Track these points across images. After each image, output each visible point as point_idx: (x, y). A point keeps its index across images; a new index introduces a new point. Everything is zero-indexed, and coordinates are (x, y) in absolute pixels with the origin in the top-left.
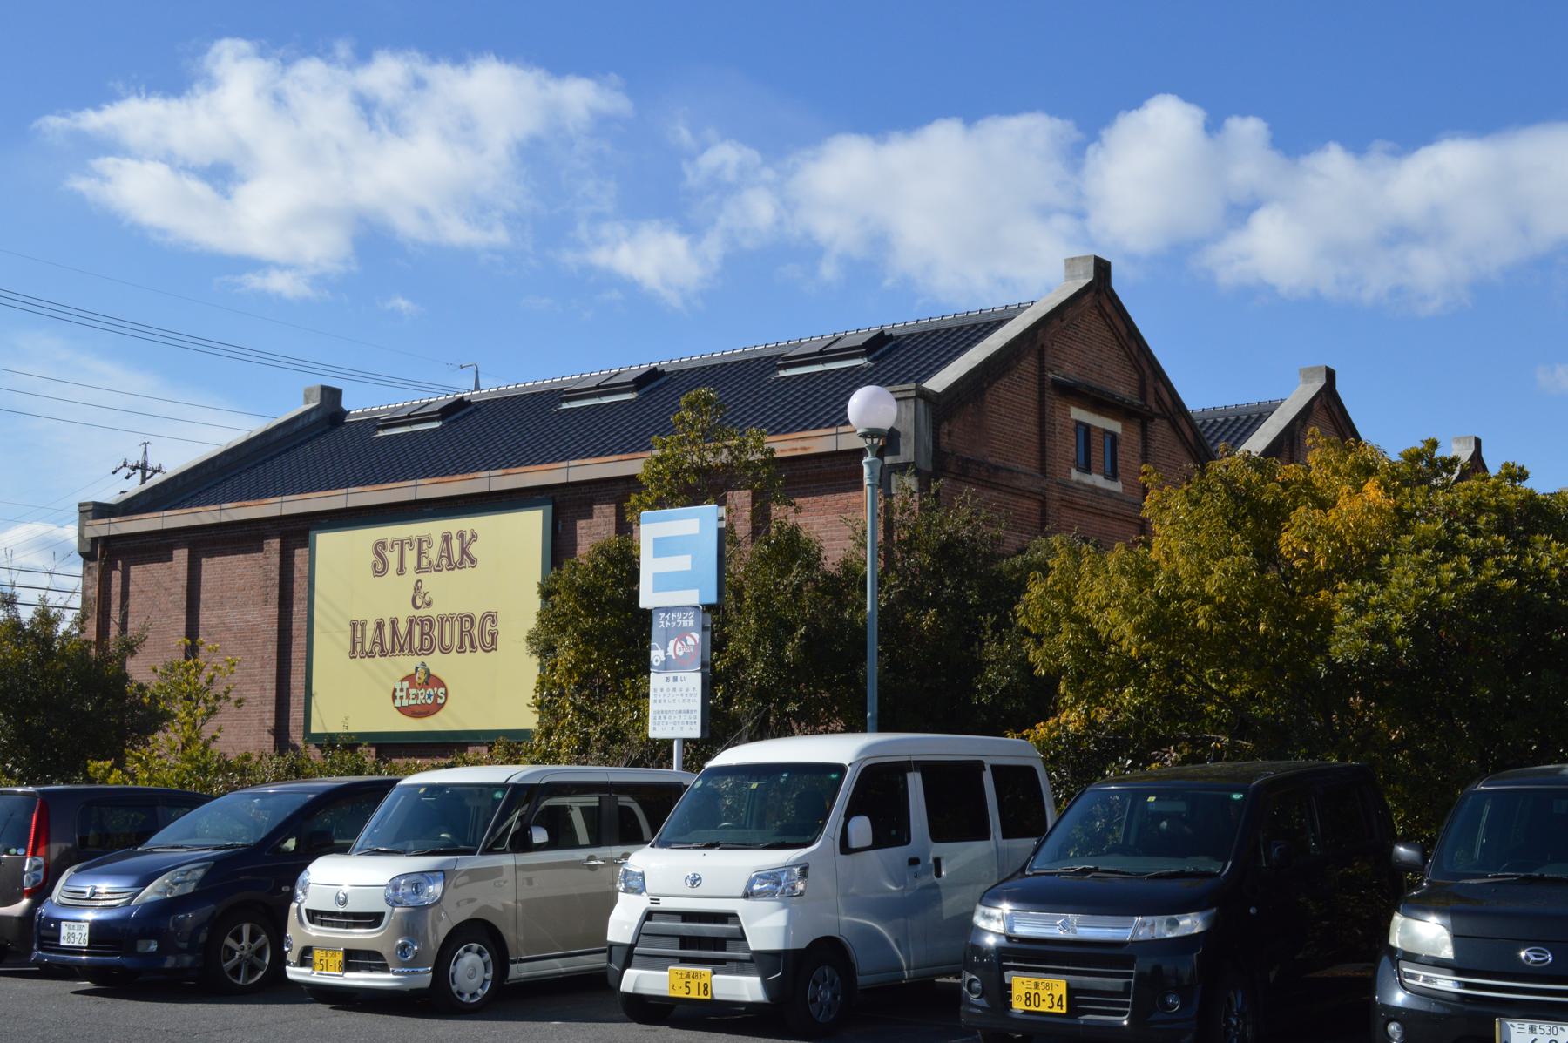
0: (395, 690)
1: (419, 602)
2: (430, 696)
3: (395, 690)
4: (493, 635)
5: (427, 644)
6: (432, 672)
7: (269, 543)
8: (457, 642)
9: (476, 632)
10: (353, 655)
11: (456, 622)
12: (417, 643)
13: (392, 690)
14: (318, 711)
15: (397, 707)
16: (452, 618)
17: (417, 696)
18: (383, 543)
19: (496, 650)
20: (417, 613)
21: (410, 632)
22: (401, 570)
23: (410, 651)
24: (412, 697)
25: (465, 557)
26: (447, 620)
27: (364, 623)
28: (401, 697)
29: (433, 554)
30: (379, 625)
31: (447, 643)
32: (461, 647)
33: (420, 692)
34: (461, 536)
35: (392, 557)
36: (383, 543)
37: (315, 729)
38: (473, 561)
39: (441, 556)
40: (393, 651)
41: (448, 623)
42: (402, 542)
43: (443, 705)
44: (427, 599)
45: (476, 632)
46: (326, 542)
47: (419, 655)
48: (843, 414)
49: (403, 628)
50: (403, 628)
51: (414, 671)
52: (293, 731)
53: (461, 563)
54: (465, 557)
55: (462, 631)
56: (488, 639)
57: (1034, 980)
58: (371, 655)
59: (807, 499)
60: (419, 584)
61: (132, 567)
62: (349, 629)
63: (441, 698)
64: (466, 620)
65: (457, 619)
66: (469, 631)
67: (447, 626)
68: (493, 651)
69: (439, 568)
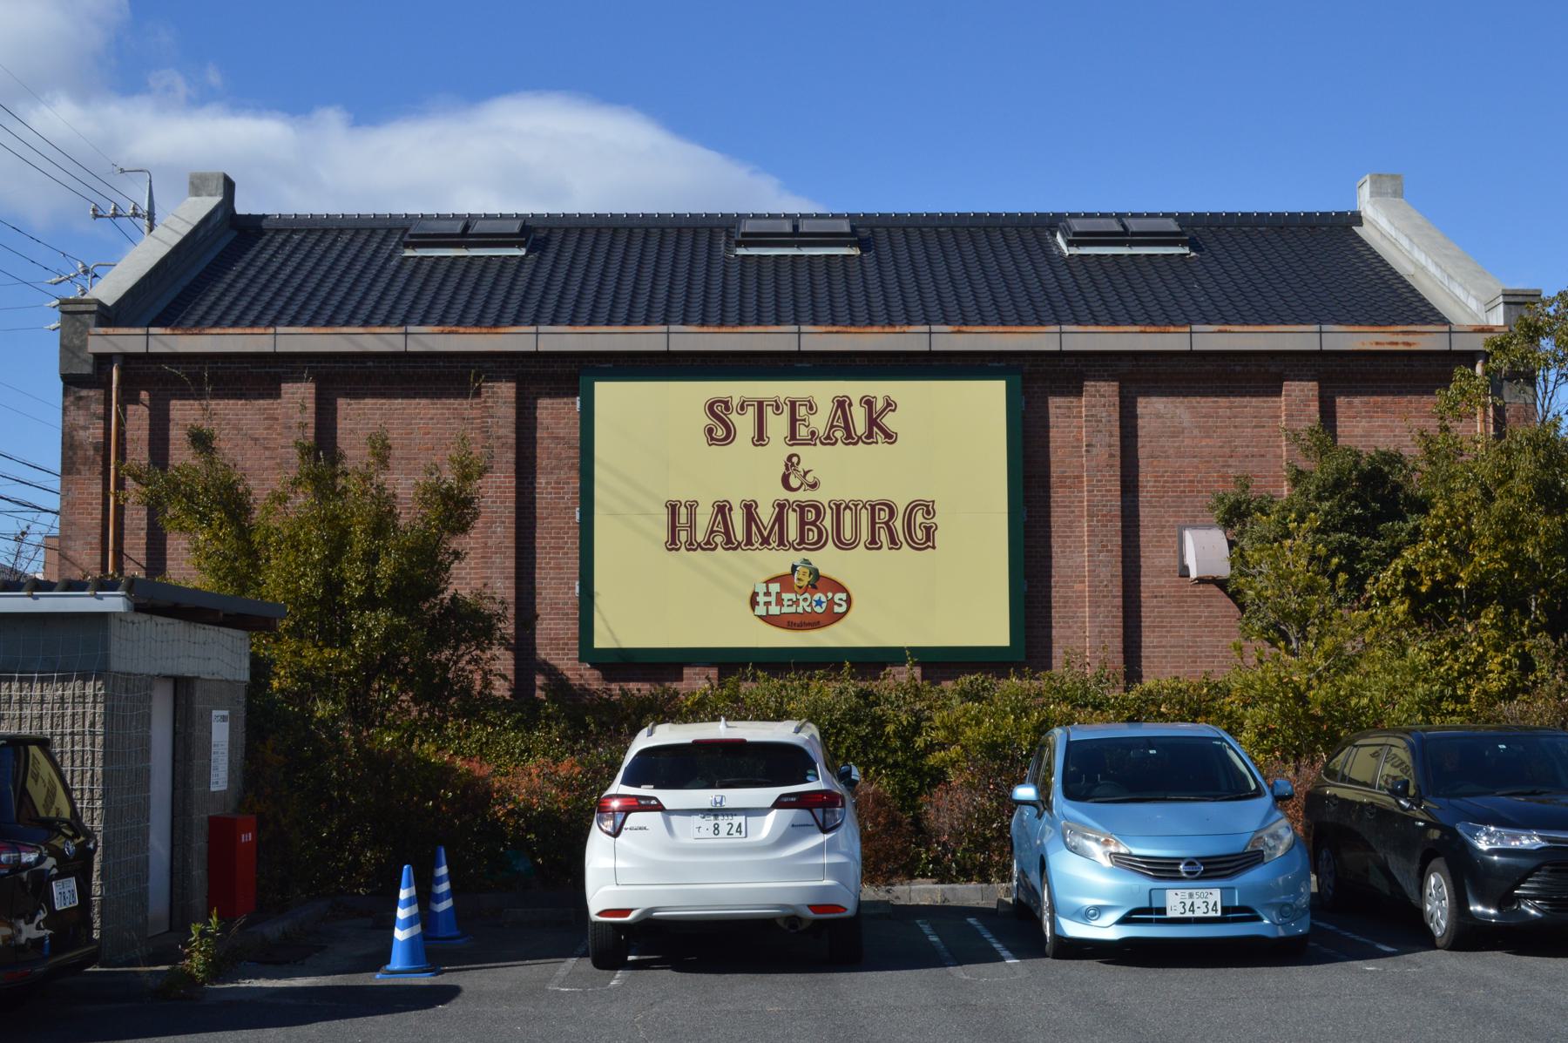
0: (755, 594)
1: (794, 482)
2: (819, 603)
3: (755, 594)
4: (929, 532)
5: (813, 536)
6: (821, 572)
7: (493, 387)
8: (865, 535)
9: (898, 524)
10: (672, 544)
11: (864, 511)
12: (793, 533)
13: (749, 593)
14: (604, 620)
15: (760, 617)
16: (856, 506)
17: (797, 602)
18: (726, 403)
19: (934, 547)
20: (792, 497)
21: (780, 519)
22: (760, 437)
23: (781, 543)
24: (785, 603)
25: (875, 429)
26: (847, 507)
27: (692, 507)
28: (767, 604)
29: (820, 422)
30: (722, 509)
31: (848, 536)
32: (873, 541)
33: (801, 598)
34: (868, 403)
35: (744, 424)
36: (726, 403)
37: (601, 641)
38: (890, 437)
39: (832, 426)
40: (749, 542)
41: (848, 511)
42: (760, 404)
43: (843, 615)
44: (810, 478)
45: (898, 524)
46: (609, 395)
47: (796, 549)
48: (1097, 305)
49: (766, 514)
50: (766, 514)
51: (789, 570)
52: (541, 644)
53: (870, 436)
54: (875, 429)
55: (873, 523)
56: (920, 534)
57: (1188, 891)
58: (708, 546)
59: (1385, 398)
60: (795, 460)
61: (173, 402)
62: (664, 516)
63: (840, 605)
64: (880, 510)
65: (864, 506)
66: (887, 523)
67: (847, 516)
68: (930, 549)
69: (829, 440)
